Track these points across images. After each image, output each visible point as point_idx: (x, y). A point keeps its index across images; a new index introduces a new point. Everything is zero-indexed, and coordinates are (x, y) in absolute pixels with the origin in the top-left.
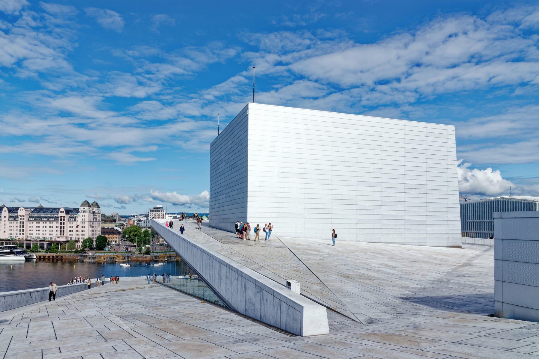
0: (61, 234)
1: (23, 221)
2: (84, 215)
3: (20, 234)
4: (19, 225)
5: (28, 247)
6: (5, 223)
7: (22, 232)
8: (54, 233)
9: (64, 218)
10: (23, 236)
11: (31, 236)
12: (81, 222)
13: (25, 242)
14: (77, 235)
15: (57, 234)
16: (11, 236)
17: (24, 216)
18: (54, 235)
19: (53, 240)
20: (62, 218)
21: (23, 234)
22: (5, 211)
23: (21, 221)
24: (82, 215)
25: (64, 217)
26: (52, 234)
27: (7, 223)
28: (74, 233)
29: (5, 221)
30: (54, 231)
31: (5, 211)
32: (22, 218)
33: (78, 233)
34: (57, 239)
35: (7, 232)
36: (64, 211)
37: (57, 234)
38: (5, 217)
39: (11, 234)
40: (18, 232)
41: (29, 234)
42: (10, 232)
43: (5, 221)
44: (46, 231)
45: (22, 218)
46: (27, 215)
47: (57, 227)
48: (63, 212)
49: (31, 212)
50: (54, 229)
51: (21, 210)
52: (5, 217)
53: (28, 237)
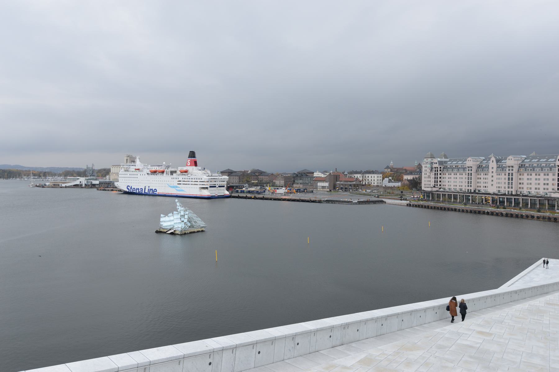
1: (512, 172)
3: (509, 187)
4: (507, 177)
5: (517, 203)
6: (492, 175)
8: (550, 187)
10: (512, 190)
11: (521, 190)
13: (513, 197)
15: (553, 189)
16: (499, 189)
17: (512, 167)
18: (550, 190)
19: (548, 196)
21: (512, 188)
23: (509, 172)
26: (547, 189)
27: (494, 174)
29: (492, 172)
30: (550, 184)
32: (511, 168)
34: (553, 195)
35: (495, 185)
37: (553, 189)
38: (493, 168)
39: (499, 187)
40: (507, 186)
41: (518, 188)
42: (498, 185)
43: (492, 172)
44: (539, 184)
45: (511, 168)
46: (517, 165)
47: (553, 180)
49: (521, 161)
50: (550, 182)
51: (509, 159)
52: (493, 168)
53: (518, 191)
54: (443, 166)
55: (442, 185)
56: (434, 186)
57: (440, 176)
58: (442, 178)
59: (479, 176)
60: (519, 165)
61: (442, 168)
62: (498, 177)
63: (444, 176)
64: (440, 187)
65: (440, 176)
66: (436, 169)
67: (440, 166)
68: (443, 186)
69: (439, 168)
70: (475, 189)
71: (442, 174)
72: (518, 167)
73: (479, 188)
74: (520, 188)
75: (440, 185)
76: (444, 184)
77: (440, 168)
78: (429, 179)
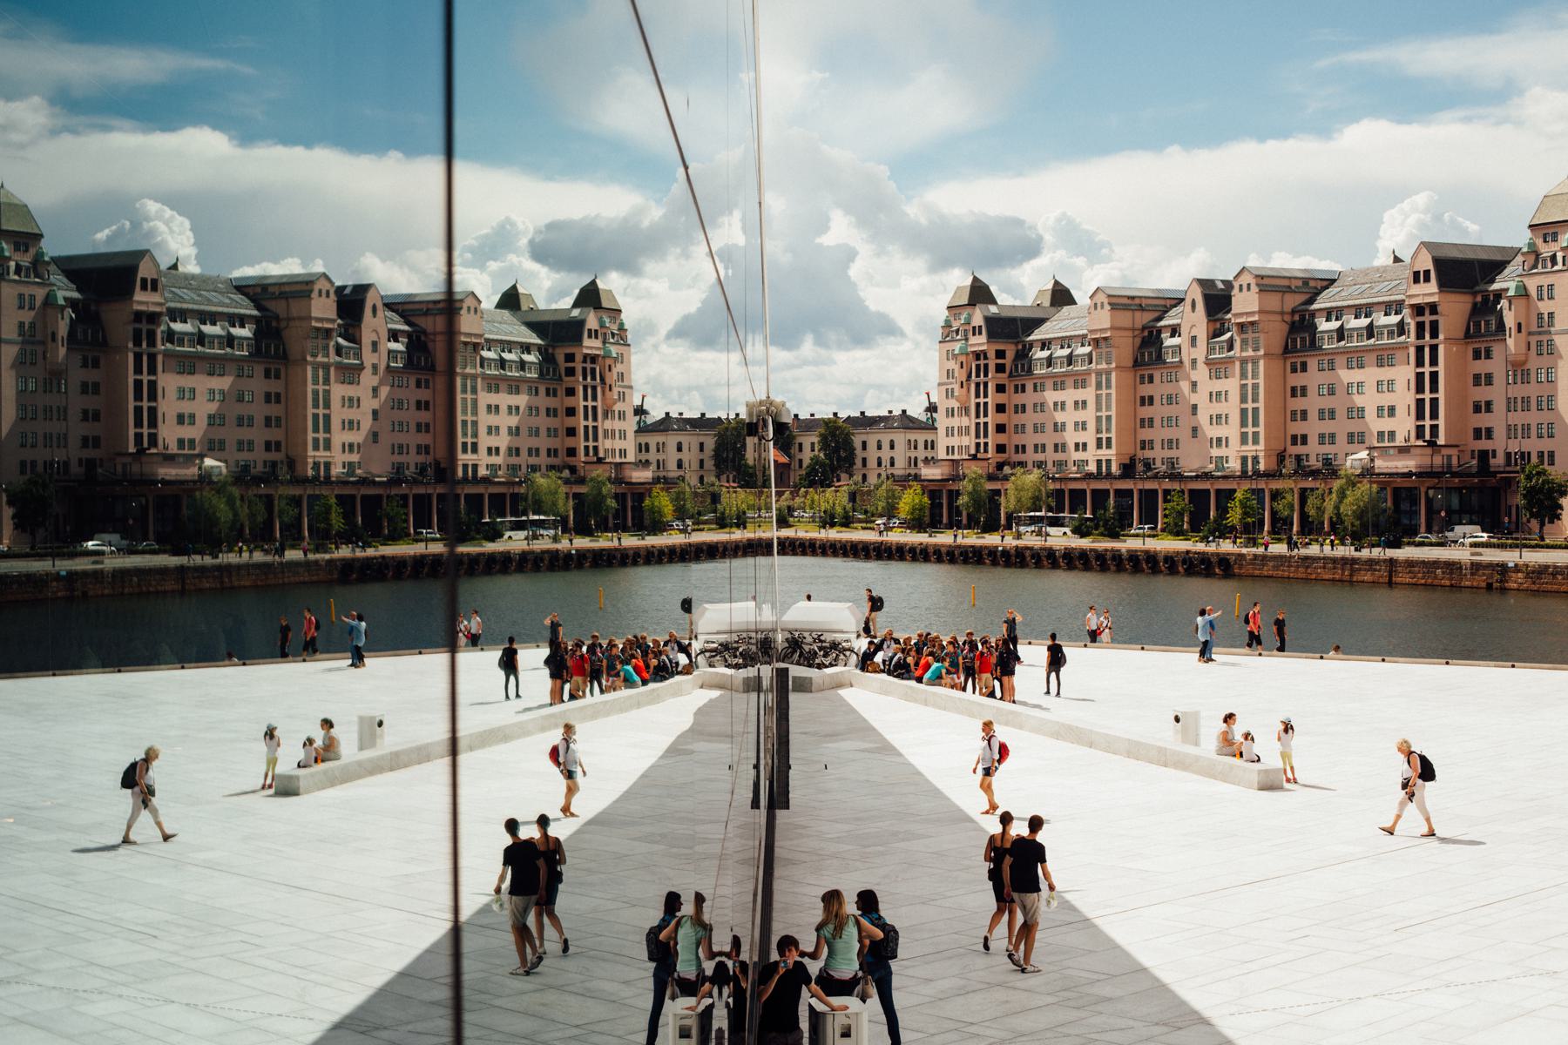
0: (1420, 431)
2: (1551, 286)
7: (1250, 430)
9: (1434, 318)
12: (1533, 340)
14: (1511, 431)
20: (1427, 318)
22: (1193, 301)
24: (1540, 288)
25: (1433, 308)
28: (1497, 421)
29: (1194, 362)
31: (1193, 301)
33: (1518, 418)
36: (1430, 266)
48: (1427, 279)
49: (1303, 298)
54: (1017, 344)
55: (1011, 449)
56: (973, 451)
57: (1002, 398)
58: (1010, 409)
59: (1146, 390)
60: (1288, 318)
61: (1010, 355)
62: (1219, 385)
63: (1019, 399)
64: (1002, 457)
65: (1002, 398)
66: (982, 362)
67: (1001, 347)
68: (1017, 452)
69: (991, 355)
70: (1132, 459)
71: (1010, 388)
72: (1286, 328)
73: (1148, 454)
74: (1294, 439)
75: (1001, 449)
76: (1018, 439)
77: (1000, 354)
78: (965, 421)
